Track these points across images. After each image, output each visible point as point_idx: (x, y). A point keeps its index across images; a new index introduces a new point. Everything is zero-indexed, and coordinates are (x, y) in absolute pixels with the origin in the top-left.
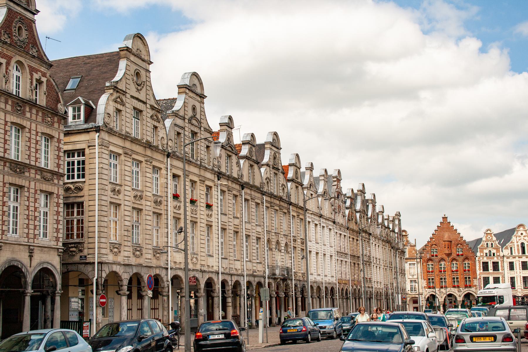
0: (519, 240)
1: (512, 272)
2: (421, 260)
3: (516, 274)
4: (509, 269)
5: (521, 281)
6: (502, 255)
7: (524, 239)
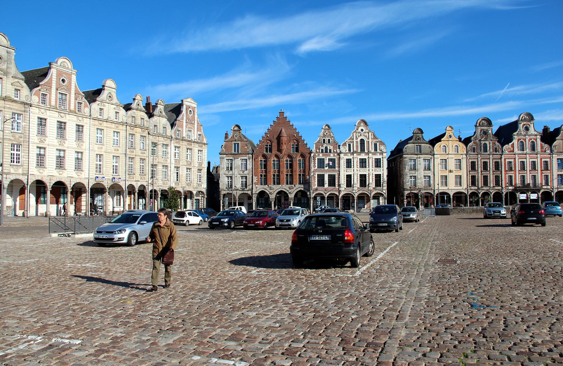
0: (359, 136)
1: (349, 169)
2: (253, 156)
3: (353, 171)
4: (345, 167)
5: (357, 179)
6: (338, 152)
7: (364, 136)
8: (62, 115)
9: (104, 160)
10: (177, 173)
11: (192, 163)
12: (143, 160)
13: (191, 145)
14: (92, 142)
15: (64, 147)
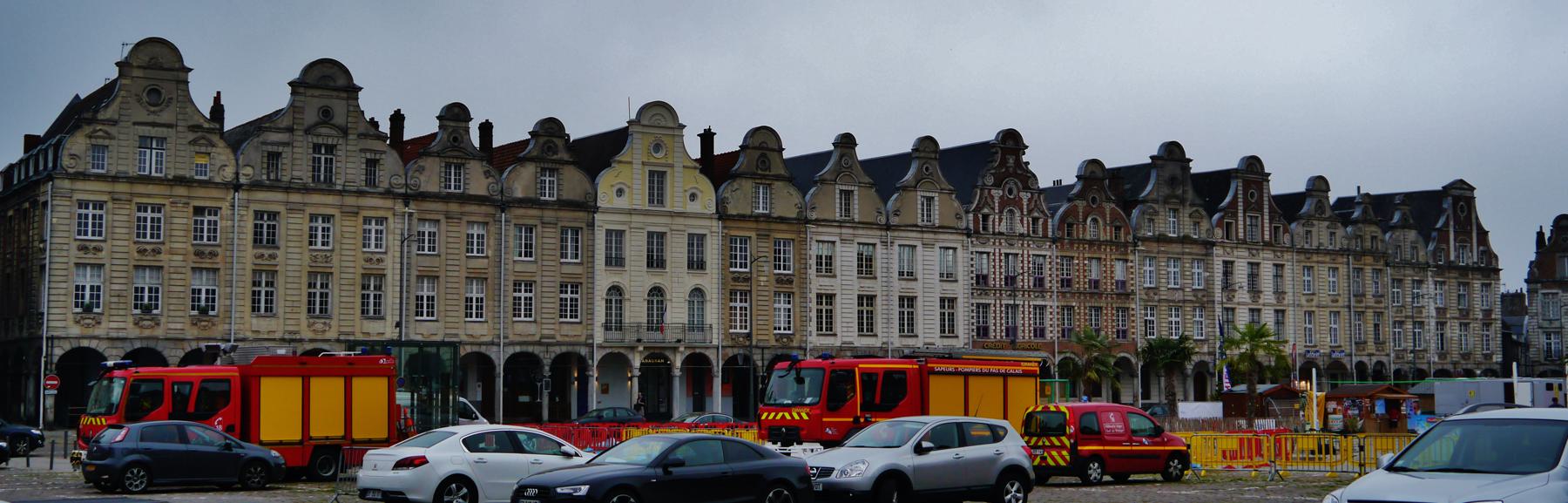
8: (1254, 252)
9: (1317, 321)
10: (1442, 335)
11: (1471, 313)
12: (1379, 314)
13: (1467, 275)
14: (1298, 291)
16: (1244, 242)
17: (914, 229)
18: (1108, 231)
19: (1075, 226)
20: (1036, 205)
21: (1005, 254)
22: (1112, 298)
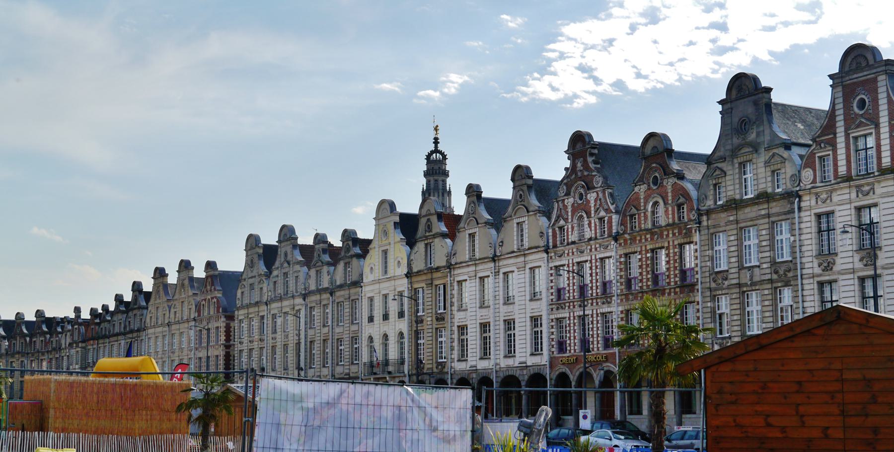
15: (834, 274)
16: (848, 178)
17: (512, 255)
18: (670, 212)
19: (637, 216)
20: (601, 205)
21: (600, 258)
22: (676, 293)
